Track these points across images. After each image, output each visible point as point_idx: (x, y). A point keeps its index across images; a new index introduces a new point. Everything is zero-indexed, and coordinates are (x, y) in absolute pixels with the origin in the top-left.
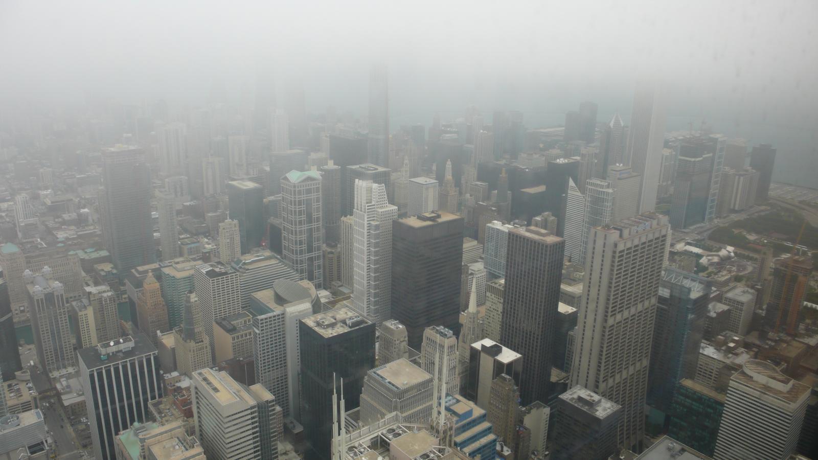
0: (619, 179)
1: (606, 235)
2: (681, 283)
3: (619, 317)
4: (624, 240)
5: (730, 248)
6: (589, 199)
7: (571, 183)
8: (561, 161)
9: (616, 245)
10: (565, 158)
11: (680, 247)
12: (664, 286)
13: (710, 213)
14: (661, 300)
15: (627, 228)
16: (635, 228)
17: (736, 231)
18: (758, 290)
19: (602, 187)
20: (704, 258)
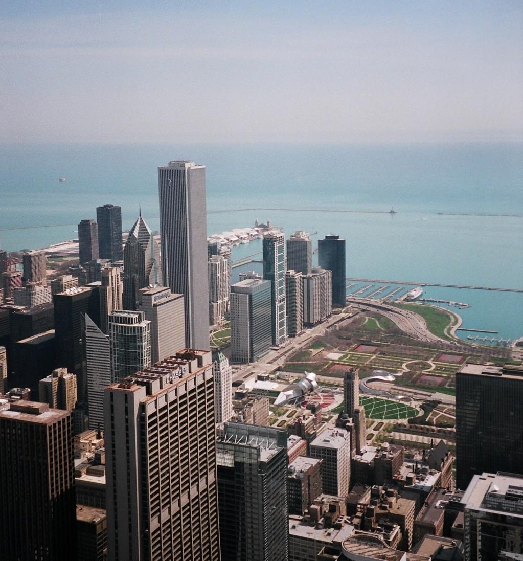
0: (155, 306)
1: (126, 396)
2: (248, 441)
3: (165, 515)
4: (154, 397)
5: (312, 376)
6: (116, 341)
7: (89, 321)
8: (72, 291)
9: (143, 407)
10: (81, 284)
11: (250, 384)
12: (225, 451)
13: (282, 333)
14: (222, 471)
15: (156, 379)
16: (168, 376)
17: (314, 352)
18: (349, 429)
19: (130, 321)
20: (282, 394)
